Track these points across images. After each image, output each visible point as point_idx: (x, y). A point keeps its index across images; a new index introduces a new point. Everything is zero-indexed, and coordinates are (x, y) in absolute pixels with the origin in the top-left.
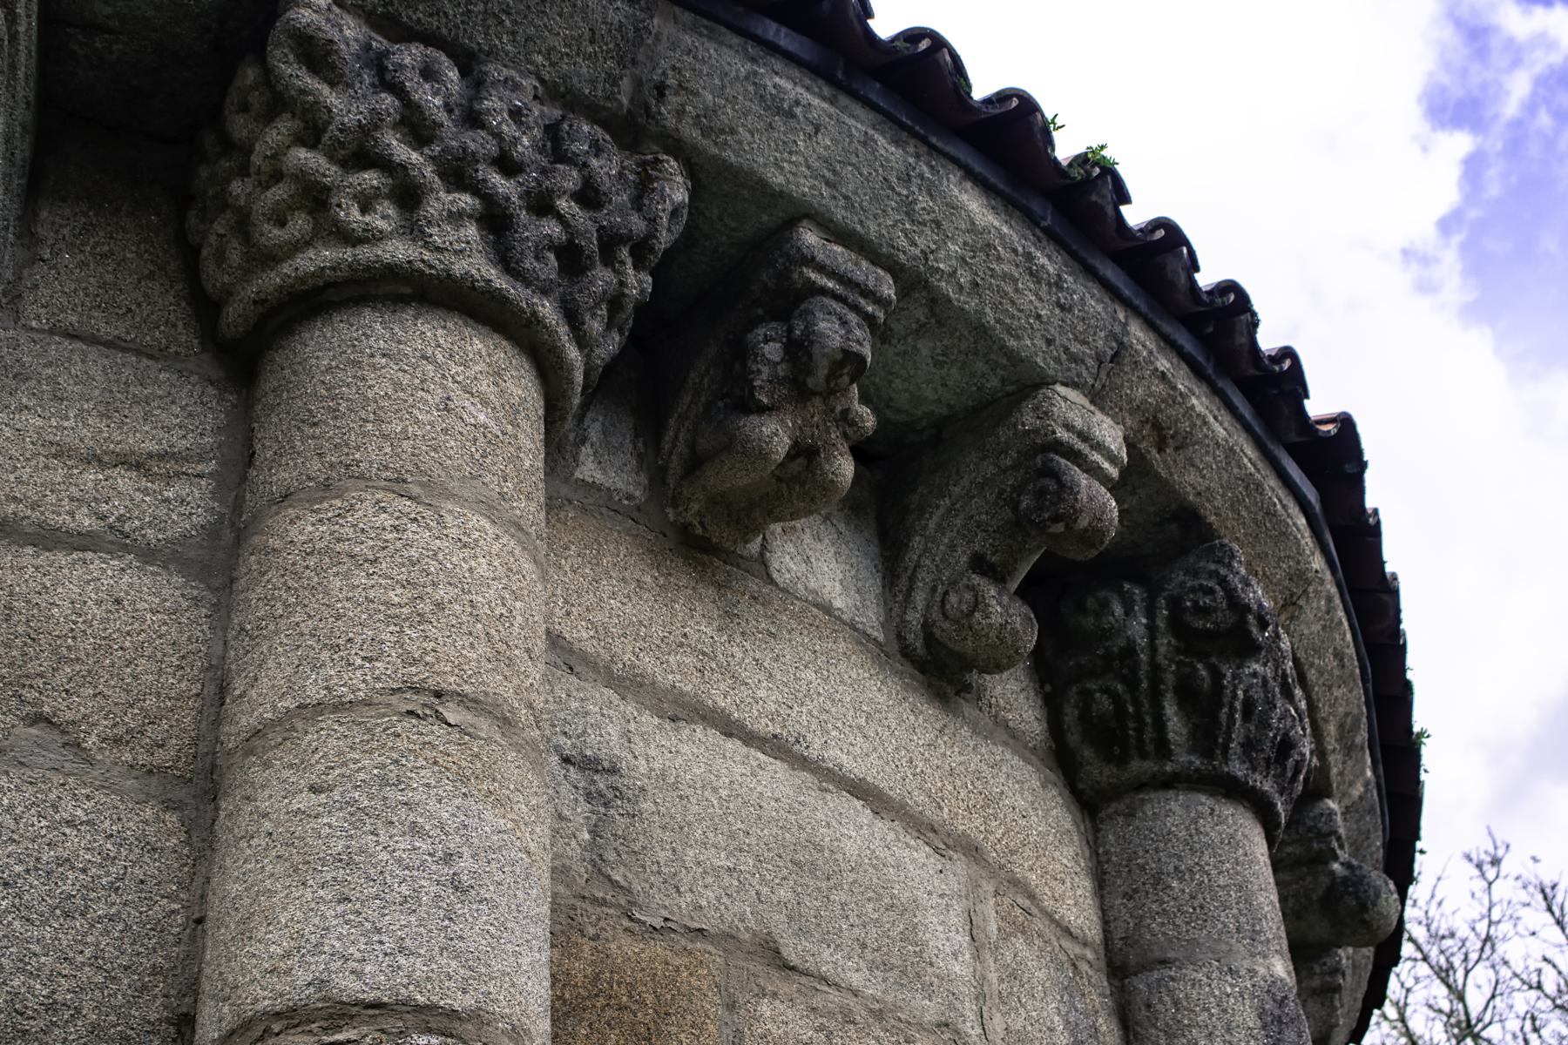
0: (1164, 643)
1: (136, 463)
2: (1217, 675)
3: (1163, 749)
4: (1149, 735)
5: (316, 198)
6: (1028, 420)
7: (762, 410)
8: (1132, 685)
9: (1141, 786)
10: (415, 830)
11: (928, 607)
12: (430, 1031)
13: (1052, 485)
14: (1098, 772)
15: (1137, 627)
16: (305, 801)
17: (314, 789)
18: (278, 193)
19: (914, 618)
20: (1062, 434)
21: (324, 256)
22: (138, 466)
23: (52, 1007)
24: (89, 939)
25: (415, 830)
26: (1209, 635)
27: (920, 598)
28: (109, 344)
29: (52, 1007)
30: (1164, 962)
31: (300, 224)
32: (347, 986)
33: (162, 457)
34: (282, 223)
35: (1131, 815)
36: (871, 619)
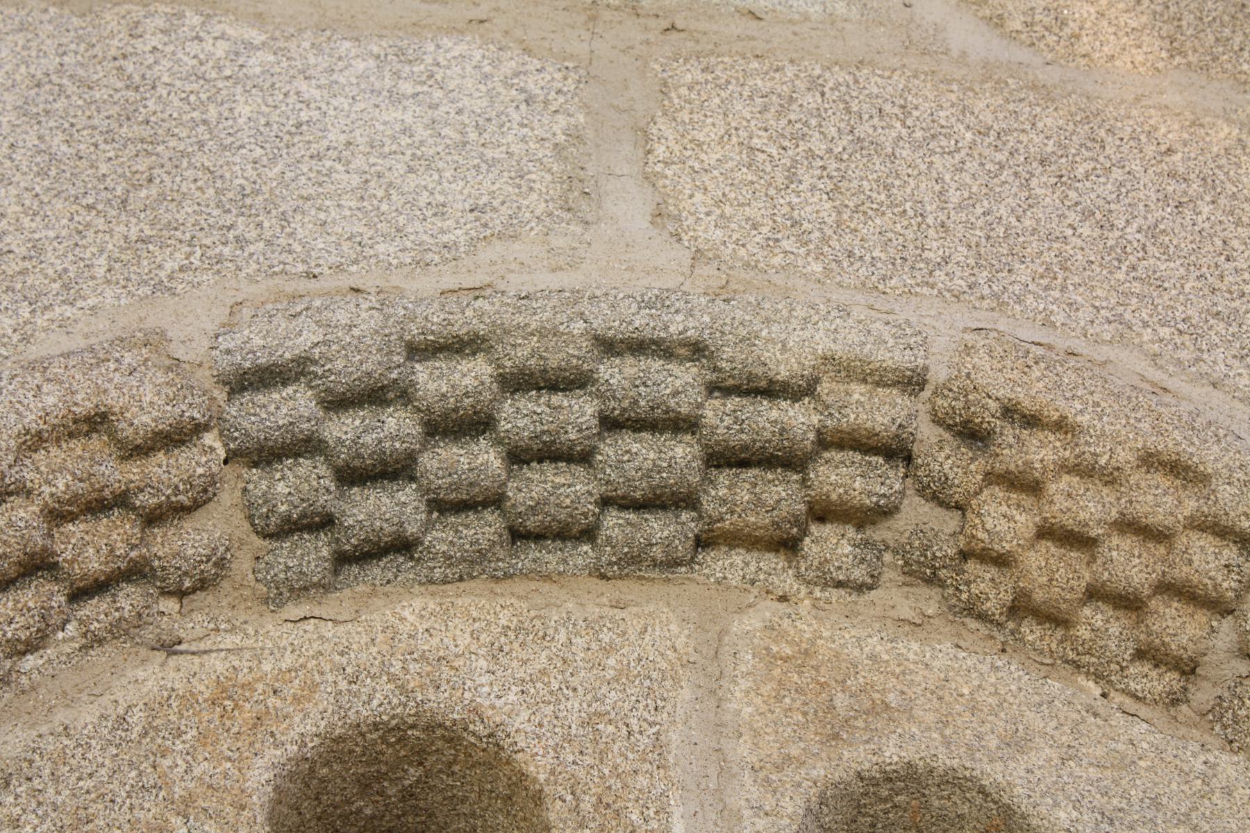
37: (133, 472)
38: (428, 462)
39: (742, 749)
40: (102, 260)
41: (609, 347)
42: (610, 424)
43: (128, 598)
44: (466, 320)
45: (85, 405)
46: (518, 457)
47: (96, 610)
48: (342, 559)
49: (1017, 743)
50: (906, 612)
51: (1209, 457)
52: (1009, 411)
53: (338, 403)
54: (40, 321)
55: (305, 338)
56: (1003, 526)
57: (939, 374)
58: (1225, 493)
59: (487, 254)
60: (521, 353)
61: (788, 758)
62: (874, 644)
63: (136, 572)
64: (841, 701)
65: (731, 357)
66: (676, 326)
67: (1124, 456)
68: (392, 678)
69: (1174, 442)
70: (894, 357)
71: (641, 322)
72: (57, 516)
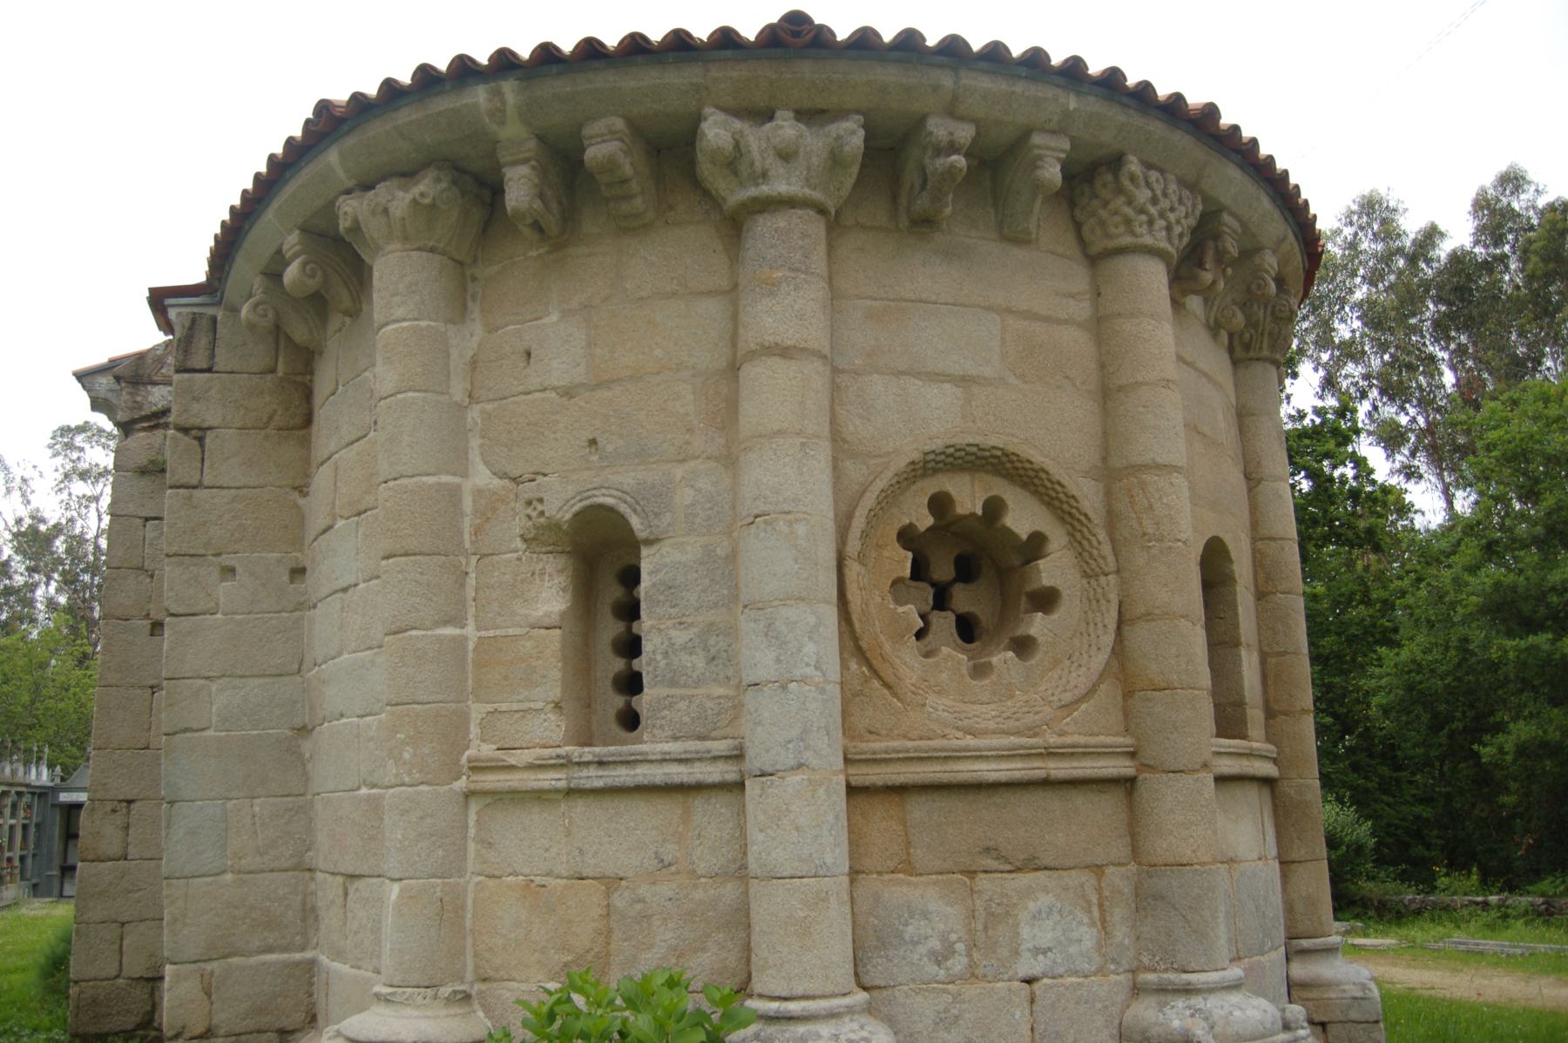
0: (1269, 319)
1: (1072, 296)
2: (1280, 329)
3: (1261, 348)
4: (1258, 346)
5: (1128, 222)
6: (1257, 260)
7: (1206, 270)
8: (1257, 331)
9: (1251, 359)
10: (1168, 419)
11: (1217, 311)
13: (1262, 282)
14: (1239, 353)
15: (1261, 313)
16: (1141, 409)
17: (1144, 407)
18: (1117, 219)
19: (1212, 315)
20: (1267, 266)
21: (1127, 240)
22: (1073, 297)
23: (1080, 456)
25: (1168, 419)
26: (1281, 319)
27: (1215, 309)
28: (1057, 255)
29: (1080, 456)
30: (1253, 414)
31: (1122, 229)
32: (1159, 460)
33: (1077, 294)
34: (1117, 228)
35: (1247, 367)
36: (1202, 317)
51: (1033, 460)
53: (936, 455)
55: (934, 447)
60: (958, 447)
65: (982, 447)
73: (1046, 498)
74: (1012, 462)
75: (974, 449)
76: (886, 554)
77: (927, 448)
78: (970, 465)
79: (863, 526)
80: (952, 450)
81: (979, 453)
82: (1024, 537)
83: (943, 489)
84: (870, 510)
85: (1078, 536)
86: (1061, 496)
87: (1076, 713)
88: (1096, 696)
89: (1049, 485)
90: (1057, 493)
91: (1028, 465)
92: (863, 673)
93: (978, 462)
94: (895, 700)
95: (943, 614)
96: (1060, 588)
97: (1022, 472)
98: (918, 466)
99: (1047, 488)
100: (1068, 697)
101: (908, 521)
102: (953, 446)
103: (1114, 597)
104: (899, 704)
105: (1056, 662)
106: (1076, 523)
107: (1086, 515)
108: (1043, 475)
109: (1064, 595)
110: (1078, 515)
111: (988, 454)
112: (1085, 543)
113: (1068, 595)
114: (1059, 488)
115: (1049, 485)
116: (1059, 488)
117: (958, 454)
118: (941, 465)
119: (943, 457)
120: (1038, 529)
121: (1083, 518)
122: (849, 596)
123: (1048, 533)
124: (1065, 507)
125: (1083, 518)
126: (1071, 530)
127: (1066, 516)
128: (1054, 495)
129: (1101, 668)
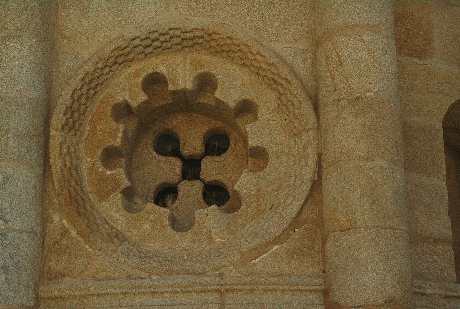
12: (368, 30)
24: (291, 13)
37: (123, 52)
38: (153, 44)
39: (187, 73)
40: (117, 24)
41: (170, 29)
42: (171, 38)
43: (125, 63)
44: (155, 29)
45: (117, 46)
46: (162, 43)
47: (122, 66)
48: (146, 55)
49: (216, 68)
50: (205, 53)
51: (233, 36)
52: (213, 32)
53: (142, 40)
54: (111, 33)
55: (138, 34)
56: (213, 45)
57: (206, 29)
58: (235, 41)
59: (157, 18)
60: (161, 31)
61: (192, 73)
62: (202, 57)
63: (125, 61)
64: (198, 65)
66: (177, 26)
67: (225, 37)
68: (152, 68)
69: (230, 35)
70: (201, 27)
71: (173, 26)
72: (116, 58)
73: (253, 69)
74: (215, 40)
75: (178, 32)
76: (99, 127)
77: (133, 35)
78: (178, 47)
79: (69, 103)
80: (156, 35)
81: (183, 36)
82: (232, 105)
83: (157, 70)
84: (75, 90)
85: (284, 99)
86: (264, 66)
87: (265, 255)
88: (289, 240)
89: (251, 57)
90: (260, 62)
91: (228, 42)
92: (64, 224)
93: (185, 43)
94: (87, 246)
95: (193, 182)
96: (267, 147)
97: (226, 48)
98: (126, 51)
99: (251, 60)
100: (257, 242)
101: (121, 99)
102: (155, 31)
103: (311, 151)
104: (90, 250)
105: (259, 213)
106: (280, 89)
107: (286, 79)
108: (245, 49)
109: (270, 153)
110: (279, 81)
111: (191, 35)
112: (289, 104)
113: (275, 152)
114: (260, 58)
115: (251, 57)
116: (260, 58)
117: (162, 38)
118: (150, 49)
119: (149, 42)
120: (247, 97)
121: (284, 83)
122: (51, 160)
123: (256, 101)
124: (269, 74)
125: (284, 83)
126: (278, 95)
127: (272, 83)
128: (257, 65)
129: (294, 214)
